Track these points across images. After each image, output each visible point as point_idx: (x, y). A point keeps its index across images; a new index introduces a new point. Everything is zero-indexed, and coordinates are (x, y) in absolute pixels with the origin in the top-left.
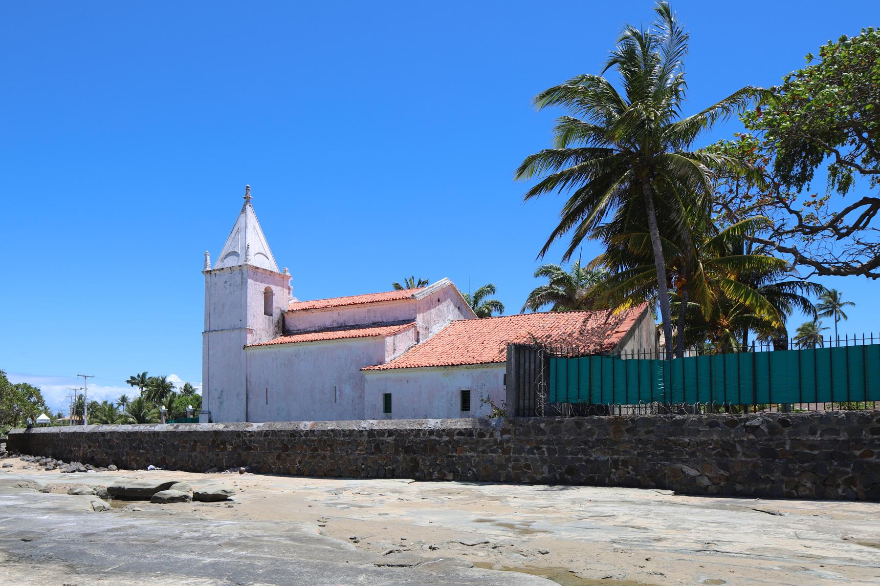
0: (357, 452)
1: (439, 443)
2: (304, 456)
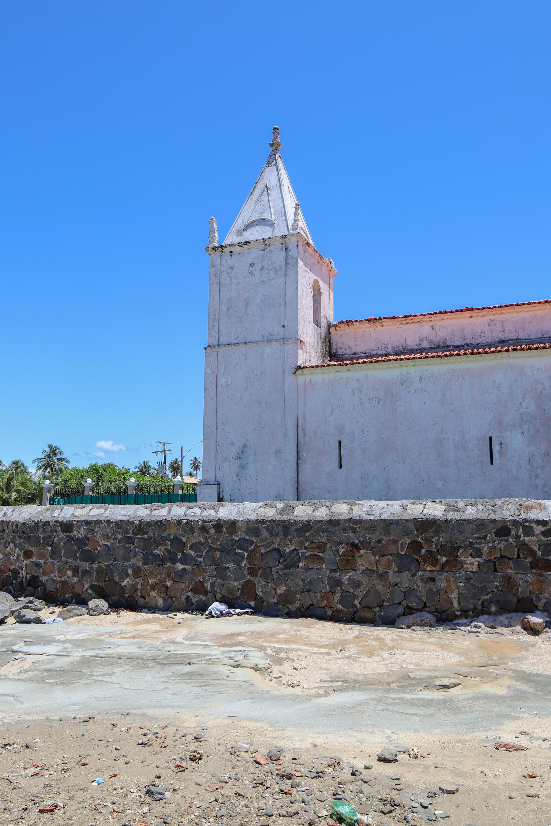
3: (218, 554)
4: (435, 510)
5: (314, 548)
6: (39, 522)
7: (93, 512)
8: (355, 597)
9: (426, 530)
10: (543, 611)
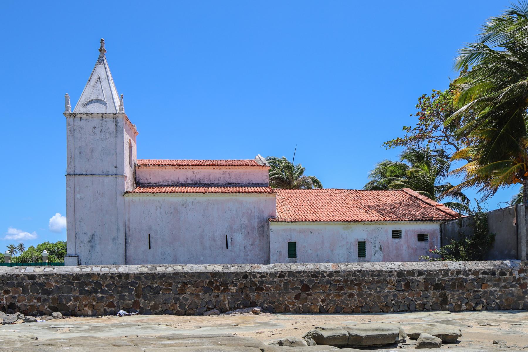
0: (387, 290)
1: (466, 280)
2: (329, 295)
3: (120, 289)
4: (219, 268)
5: (167, 285)
6: (13, 275)
7: (48, 270)
8: (186, 305)
9: (215, 277)
10: (259, 306)
